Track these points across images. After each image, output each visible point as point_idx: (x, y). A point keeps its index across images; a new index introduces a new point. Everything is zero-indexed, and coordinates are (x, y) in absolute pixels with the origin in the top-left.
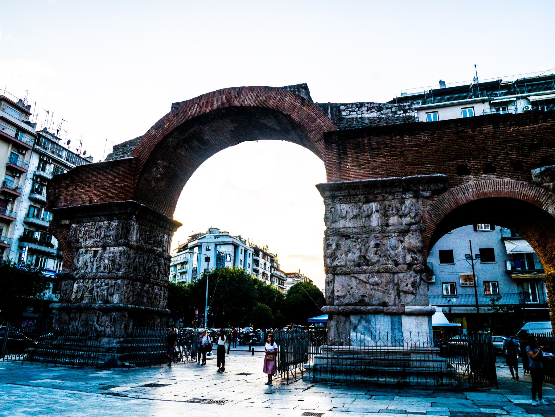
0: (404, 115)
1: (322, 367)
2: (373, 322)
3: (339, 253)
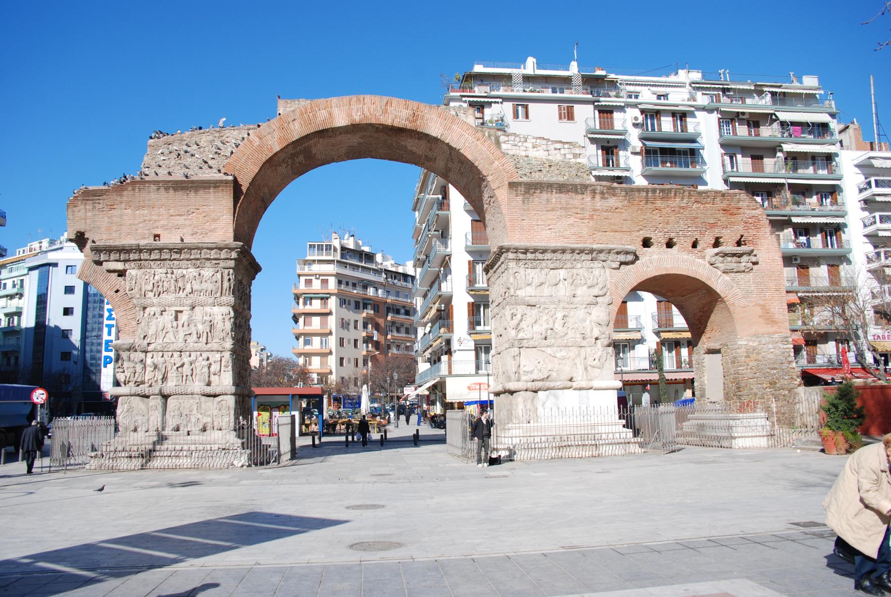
3: (523, 325)
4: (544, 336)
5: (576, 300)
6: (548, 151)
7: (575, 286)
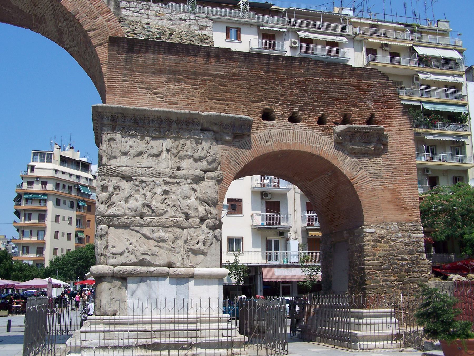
0: (200, 32)
1: (92, 343)
3: (115, 198)
6: (172, 20)
7: (181, 158)
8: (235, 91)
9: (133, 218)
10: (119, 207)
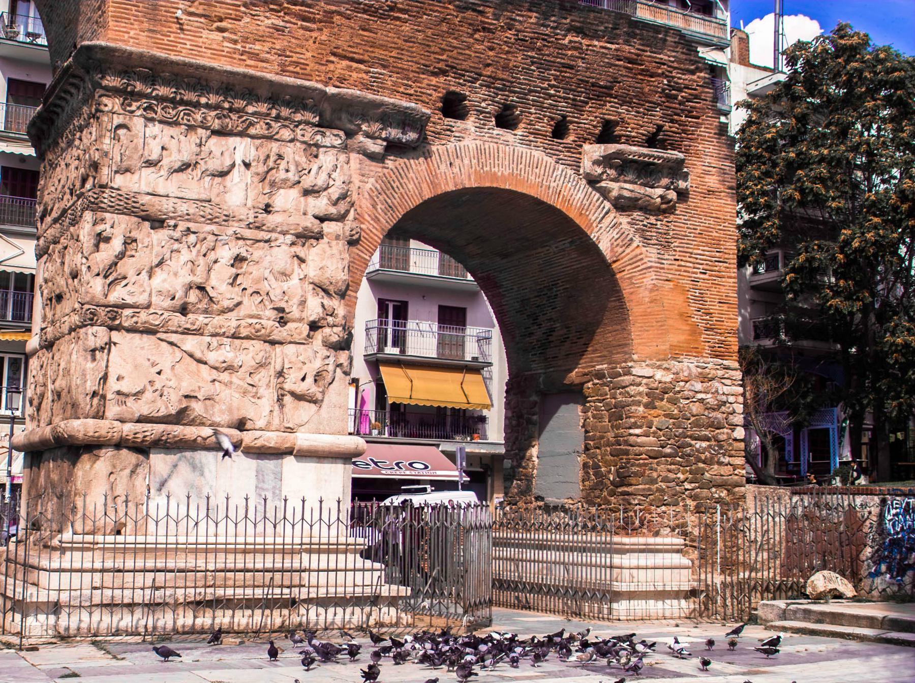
2: (210, 471)
3: (127, 267)
4: (178, 303)
5: (272, 220)
7: (273, 184)
8: (393, 45)
9: (166, 314)
10: (136, 285)
